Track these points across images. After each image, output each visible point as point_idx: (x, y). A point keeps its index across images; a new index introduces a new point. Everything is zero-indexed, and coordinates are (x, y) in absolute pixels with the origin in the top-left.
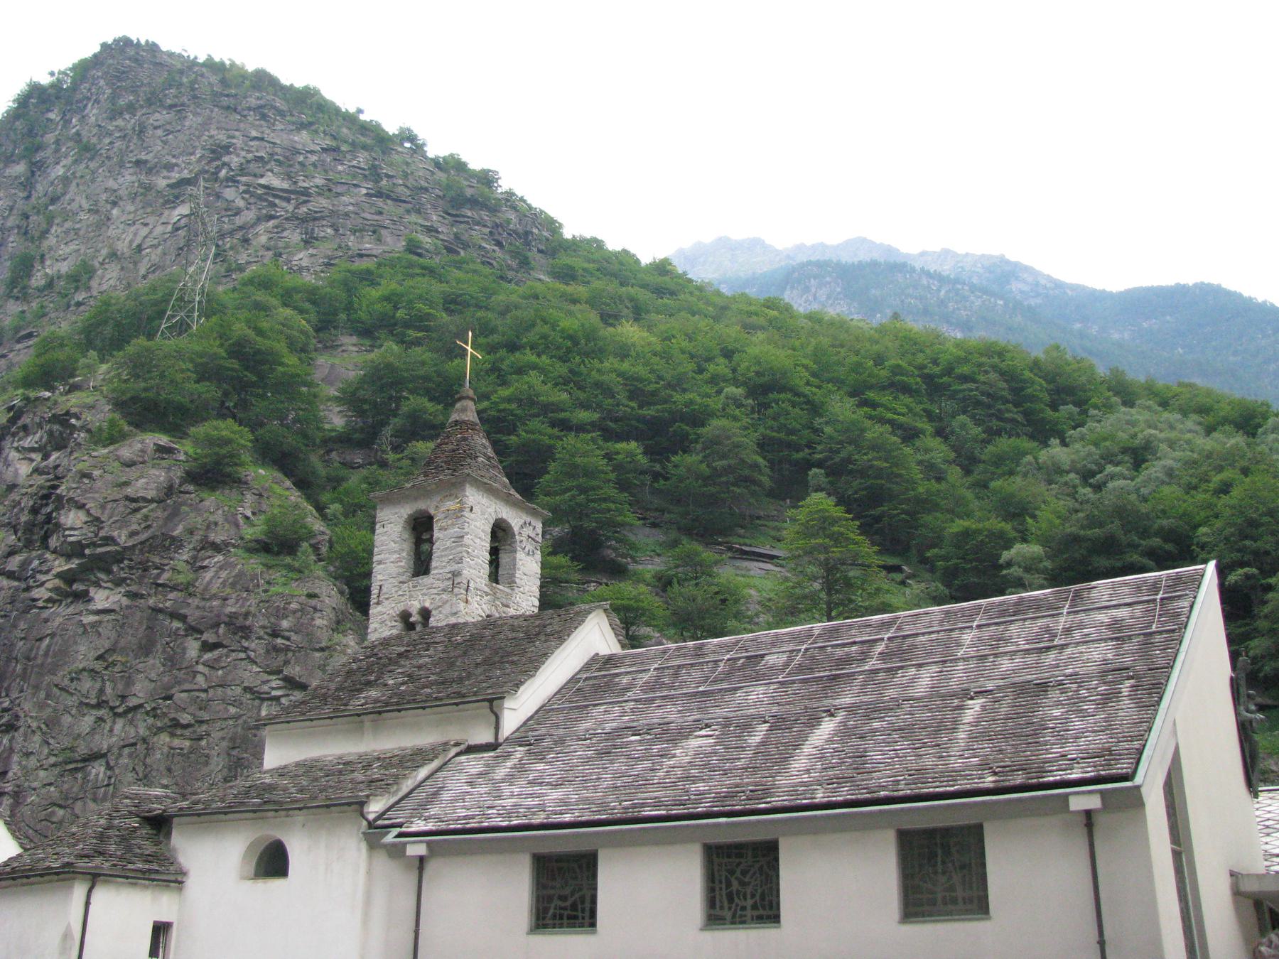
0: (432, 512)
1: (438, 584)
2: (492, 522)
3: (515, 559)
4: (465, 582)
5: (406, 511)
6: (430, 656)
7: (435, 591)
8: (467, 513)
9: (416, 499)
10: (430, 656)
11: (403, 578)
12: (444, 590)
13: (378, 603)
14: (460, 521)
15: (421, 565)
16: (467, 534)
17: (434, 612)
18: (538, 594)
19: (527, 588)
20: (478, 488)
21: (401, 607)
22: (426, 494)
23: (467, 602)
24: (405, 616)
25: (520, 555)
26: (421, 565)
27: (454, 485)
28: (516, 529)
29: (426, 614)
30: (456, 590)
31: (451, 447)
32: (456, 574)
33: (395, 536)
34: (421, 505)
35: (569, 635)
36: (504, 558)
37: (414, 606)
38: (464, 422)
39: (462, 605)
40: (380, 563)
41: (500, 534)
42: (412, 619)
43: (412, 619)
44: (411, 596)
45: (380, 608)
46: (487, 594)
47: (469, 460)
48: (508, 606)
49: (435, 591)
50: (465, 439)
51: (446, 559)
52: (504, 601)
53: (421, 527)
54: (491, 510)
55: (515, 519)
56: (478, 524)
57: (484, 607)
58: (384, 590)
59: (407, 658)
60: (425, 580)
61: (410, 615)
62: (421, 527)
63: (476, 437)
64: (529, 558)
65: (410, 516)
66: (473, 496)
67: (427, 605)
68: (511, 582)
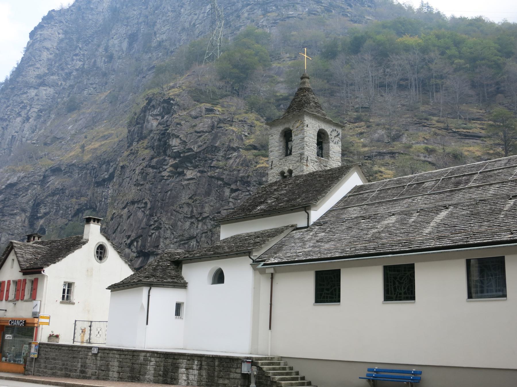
0: (291, 128)
1: (295, 159)
2: (317, 130)
3: (329, 146)
4: (306, 157)
5: (280, 129)
6: (286, 190)
7: (294, 162)
8: (305, 128)
9: (284, 123)
10: (286, 190)
11: (282, 157)
12: (297, 161)
13: (271, 169)
14: (303, 131)
15: (288, 152)
16: (306, 137)
17: (294, 171)
18: (340, 161)
19: (335, 158)
20: (310, 116)
21: (280, 170)
22: (289, 121)
23: (307, 165)
24: (282, 173)
25: (331, 144)
26: (288, 152)
27: (299, 116)
28: (329, 133)
29: (290, 172)
30: (302, 161)
31: (298, 100)
32: (302, 154)
33: (277, 140)
34: (286, 126)
35: (341, 178)
36: (325, 146)
37: (286, 169)
38: (304, 88)
39: (305, 167)
40: (271, 152)
41: (322, 136)
42: (285, 175)
43: (285, 175)
44: (284, 165)
45: (272, 171)
46: (316, 162)
47: (306, 105)
48: (326, 166)
49: (294, 162)
50: (304, 96)
51: (298, 148)
52: (325, 164)
53: (287, 135)
54: (317, 125)
55: (328, 129)
56: (311, 132)
57: (315, 167)
58: (274, 163)
59: (277, 191)
60: (290, 158)
61: (284, 173)
62: (287, 135)
63: (310, 94)
64: (335, 145)
65: (283, 131)
66: (308, 120)
67: (291, 168)
68: (328, 156)
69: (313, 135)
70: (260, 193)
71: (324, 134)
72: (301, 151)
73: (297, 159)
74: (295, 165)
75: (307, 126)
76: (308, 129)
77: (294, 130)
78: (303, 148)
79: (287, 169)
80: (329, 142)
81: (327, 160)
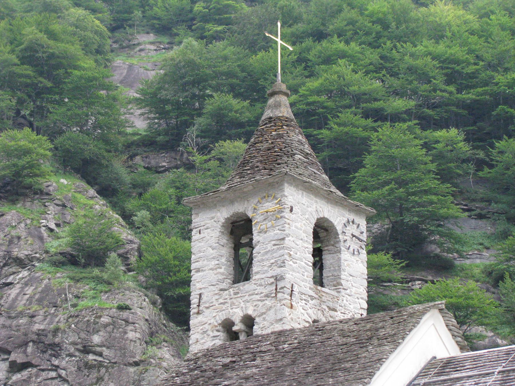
0: (250, 214)
1: (260, 289)
2: (314, 221)
3: (339, 259)
4: (289, 286)
5: (224, 214)
6: (257, 366)
7: (258, 297)
8: (286, 214)
9: (232, 202)
10: (257, 366)
11: (224, 286)
12: (267, 296)
13: (198, 313)
14: (281, 222)
15: (242, 271)
16: (288, 235)
17: (257, 320)
18: (365, 295)
19: (354, 290)
20: (297, 186)
21: (221, 317)
22: (244, 197)
23: (292, 307)
24: (227, 326)
25: (345, 255)
26: (242, 271)
27: (271, 185)
28: (339, 228)
29: (249, 322)
30: (279, 295)
31: (266, 145)
32: (278, 279)
33: (213, 241)
34: (239, 208)
35: (403, 338)
36: (328, 259)
37: (237, 316)
38: (279, 118)
39: (287, 310)
40: (198, 270)
41: (322, 234)
42: (235, 328)
43: (235, 328)
44: (233, 304)
45: (200, 318)
46: (312, 298)
47: (285, 159)
48: (335, 310)
49: (258, 297)
50: (280, 136)
51: (267, 263)
52: (331, 304)
53: (240, 231)
54: (312, 209)
55: (337, 217)
56: (299, 225)
57: (310, 311)
58: (204, 298)
59: (233, 369)
60: (246, 287)
61: (233, 324)
62: (240, 231)
63: (291, 134)
64: (354, 259)
65: (227, 219)
66: (291, 195)
67: (250, 312)
68: (337, 285)
69: (305, 232)
70: (183, 374)
71: (326, 230)
72: (277, 271)
73: (266, 291)
74: (260, 304)
75: (291, 210)
76: (292, 216)
77: (257, 219)
78: (282, 265)
79: (241, 314)
80: (339, 252)
81: (334, 293)
